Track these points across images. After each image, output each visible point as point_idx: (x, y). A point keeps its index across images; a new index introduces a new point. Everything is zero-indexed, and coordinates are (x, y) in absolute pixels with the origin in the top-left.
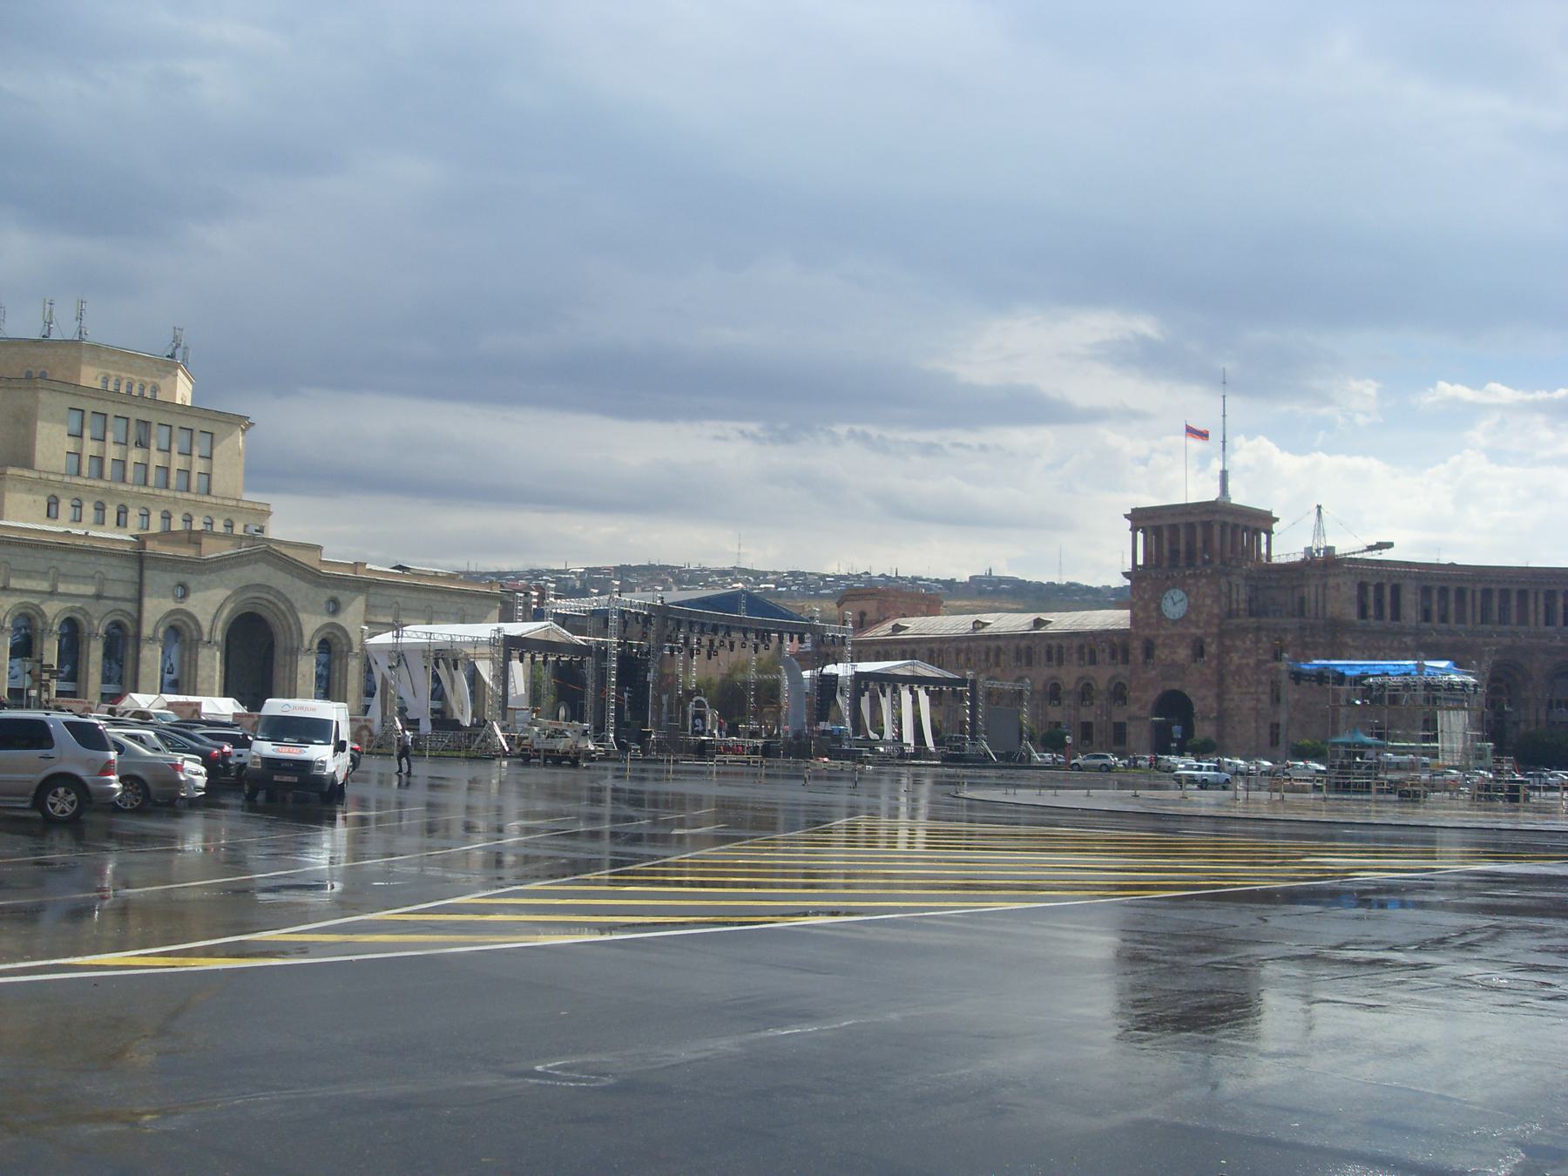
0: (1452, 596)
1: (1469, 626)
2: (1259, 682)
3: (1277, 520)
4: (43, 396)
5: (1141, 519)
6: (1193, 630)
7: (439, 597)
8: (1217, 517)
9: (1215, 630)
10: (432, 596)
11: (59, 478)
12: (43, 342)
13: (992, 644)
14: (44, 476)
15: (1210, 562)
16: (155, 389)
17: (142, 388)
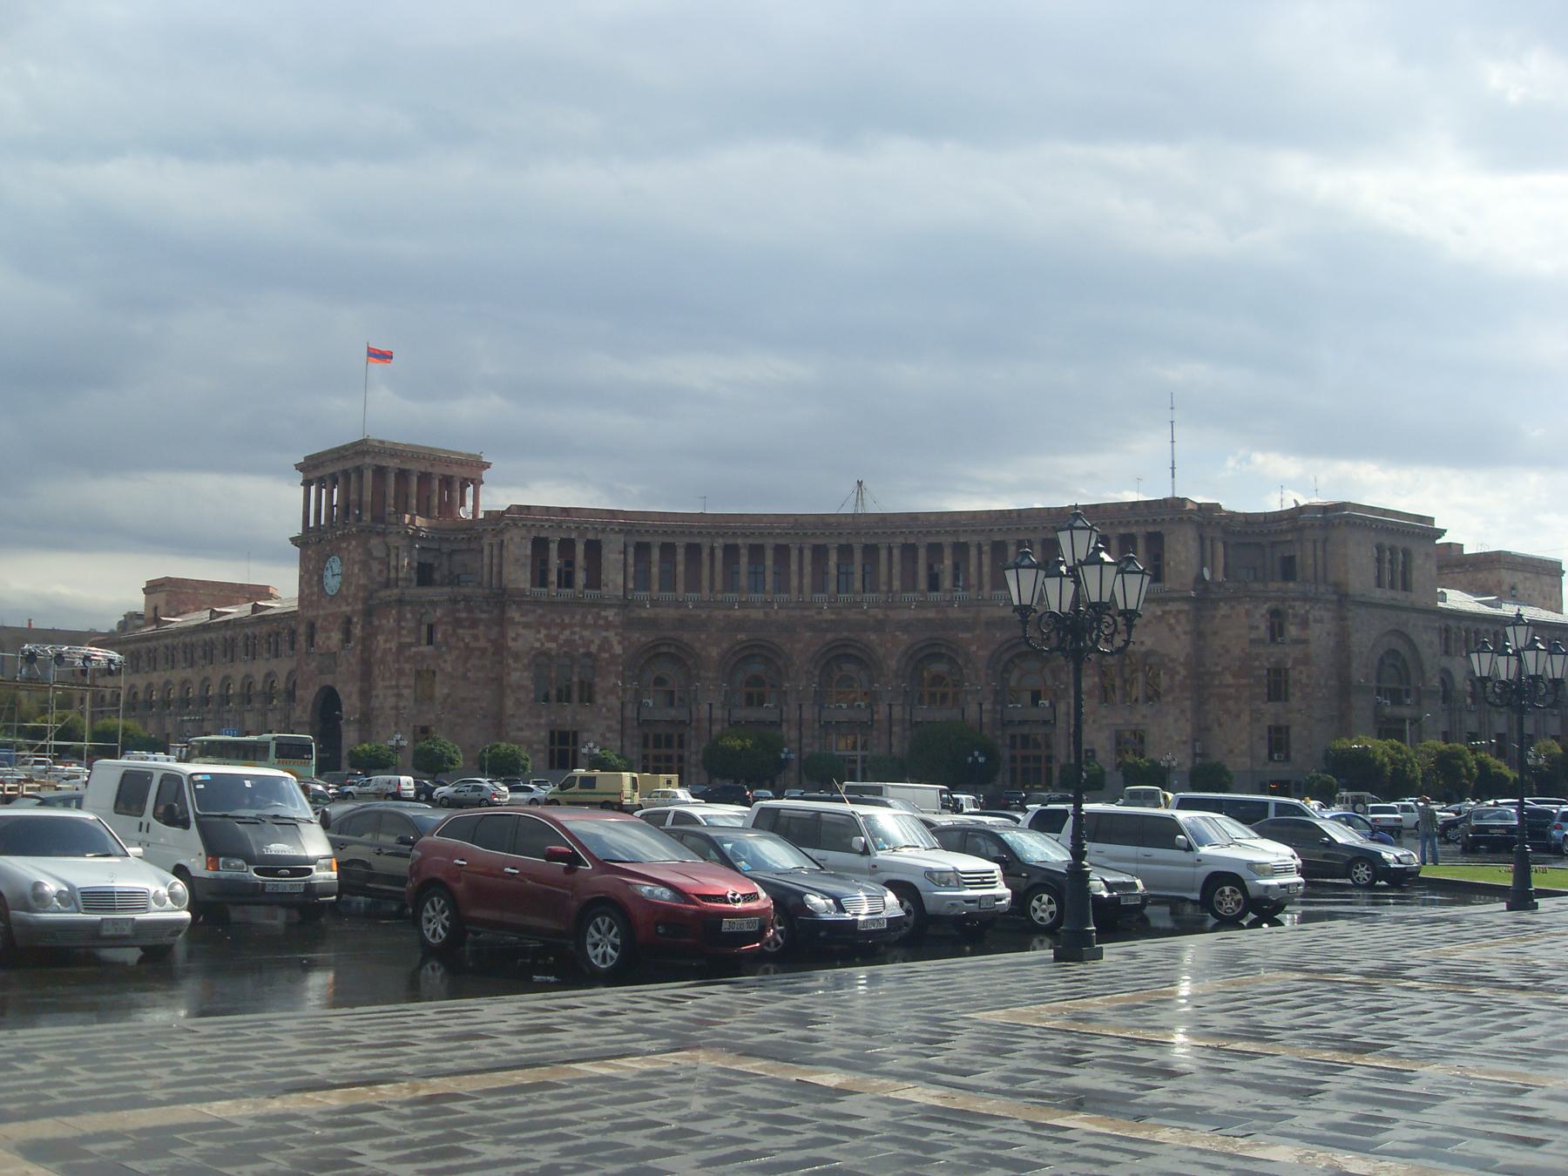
0: (680, 556)
1: (706, 593)
2: (400, 672)
3: (488, 465)
5: (315, 471)
6: (345, 608)
8: (368, 460)
9: (359, 606)
13: (207, 636)
15: (359, 518)
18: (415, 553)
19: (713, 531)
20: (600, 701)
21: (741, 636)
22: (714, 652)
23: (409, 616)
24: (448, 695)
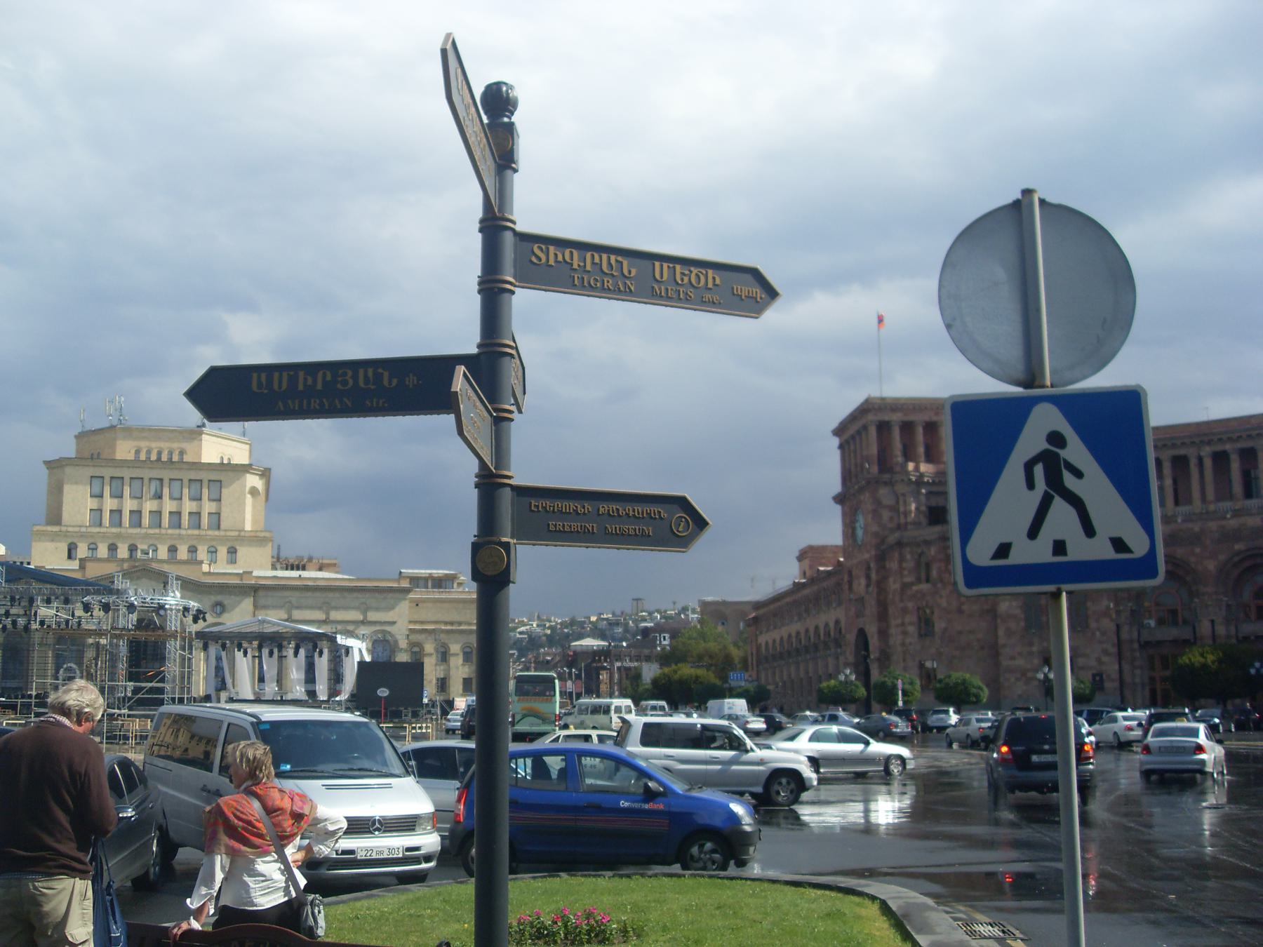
1: (1197, 505)
2: (905, 611)
4: (68, 470)
7: (337, 595)
8: (871, 417)
9: (873, 553)
10: (331, 595)
11: (77, 529)
12: (112, 427)
14: (64, 529)
16: (182, 453)
17: (171, 453)
18: (923, 499)
19: (1197, 440)
20: (1093, 625)
21: (1238, 547)
22: (1211, 566)
23: (908, 557)
24: (946, 629)
